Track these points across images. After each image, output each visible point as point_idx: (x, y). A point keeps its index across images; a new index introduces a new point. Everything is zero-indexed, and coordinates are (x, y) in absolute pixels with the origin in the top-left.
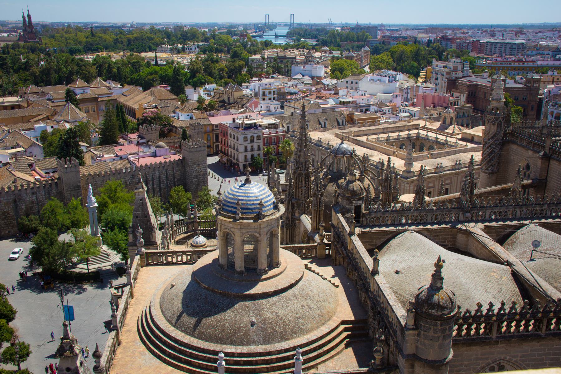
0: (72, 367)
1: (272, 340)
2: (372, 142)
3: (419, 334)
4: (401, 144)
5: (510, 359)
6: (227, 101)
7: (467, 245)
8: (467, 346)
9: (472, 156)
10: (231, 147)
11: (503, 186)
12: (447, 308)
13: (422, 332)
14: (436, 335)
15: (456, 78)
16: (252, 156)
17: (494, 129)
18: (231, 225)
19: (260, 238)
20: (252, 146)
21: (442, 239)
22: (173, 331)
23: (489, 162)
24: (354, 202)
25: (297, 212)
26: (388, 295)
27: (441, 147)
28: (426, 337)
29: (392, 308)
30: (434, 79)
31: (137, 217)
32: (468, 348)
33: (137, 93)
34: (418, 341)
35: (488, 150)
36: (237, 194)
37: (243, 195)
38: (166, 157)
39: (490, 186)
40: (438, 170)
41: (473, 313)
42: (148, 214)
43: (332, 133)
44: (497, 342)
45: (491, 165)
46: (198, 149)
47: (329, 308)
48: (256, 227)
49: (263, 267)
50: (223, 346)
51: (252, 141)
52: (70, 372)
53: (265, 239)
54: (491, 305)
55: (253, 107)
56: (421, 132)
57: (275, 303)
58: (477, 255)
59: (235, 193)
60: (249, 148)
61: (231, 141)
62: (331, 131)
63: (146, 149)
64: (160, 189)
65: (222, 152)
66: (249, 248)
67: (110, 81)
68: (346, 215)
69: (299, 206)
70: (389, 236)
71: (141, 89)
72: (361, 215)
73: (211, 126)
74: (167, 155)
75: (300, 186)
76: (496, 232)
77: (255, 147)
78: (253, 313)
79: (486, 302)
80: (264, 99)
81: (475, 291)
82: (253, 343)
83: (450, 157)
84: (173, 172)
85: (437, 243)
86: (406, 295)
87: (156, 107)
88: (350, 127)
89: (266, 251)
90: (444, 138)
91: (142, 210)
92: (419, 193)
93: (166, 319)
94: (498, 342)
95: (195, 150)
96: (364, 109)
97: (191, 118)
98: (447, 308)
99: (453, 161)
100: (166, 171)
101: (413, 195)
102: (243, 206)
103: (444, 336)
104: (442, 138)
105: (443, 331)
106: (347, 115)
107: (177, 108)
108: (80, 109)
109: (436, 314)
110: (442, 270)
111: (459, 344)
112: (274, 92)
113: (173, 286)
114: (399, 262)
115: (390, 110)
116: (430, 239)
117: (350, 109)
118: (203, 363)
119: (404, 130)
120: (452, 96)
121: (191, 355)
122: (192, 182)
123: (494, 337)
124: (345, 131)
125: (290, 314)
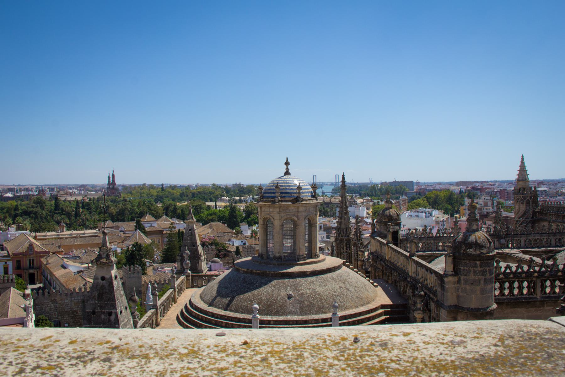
0: (107, 277)
1: (310, 311)
3: (459, 281)
13: (462, 277)
14: (477, 278)
28: (466, 281)
34: (458, 289)
49: (301, 253)
52: (104, 281)
75: (342, 251)
82: (290, 313)
98: (485, 247)
103: (485, 279)
105: (483, 273)
109: (474, 253)
125: (327, 292)
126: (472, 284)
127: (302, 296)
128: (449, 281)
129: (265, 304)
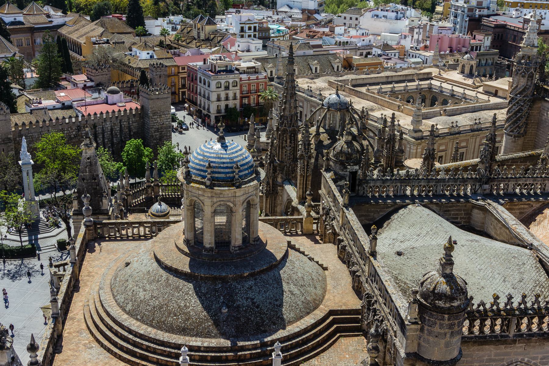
2: (374, 93)
3: (422, 330)
4: (408, 98)
5: (528, 361)
6: (196, 37)
7: (483, 223)
8: (479, 345)
9: (495, 114)
10: (200, 95)
11: (530, 153)
12: (457, 299)
13: (426, 327)
14: (442, 331)
15: (481, 16)
16: (227, 106)
17: (523, 82)
18: (200, 192)
19: (234, 210)
20: (227, 94)
21: (453, 214)
22: (126, 320)
23: (515, 122)
24: (349, 167)
25: (280, 176)
26: (386, 281)
27: (457, 101)
28: (430, 333)
29: (390, 297)
30: (452, 18)
31: (83, 179)
32: (480, 347)
33: (83, 22)
34: (420, 337)
35: (514, 107)
36: (208, 155)
37: (215, 155)
38: (120, 105)
39: (515, 152)
40: (453, 130)
41: (488, 306)
42: (98, 175)
43: (325, 81)
44: (514, 342)
45: (518, 126)
46: (159, 97)
47: (316, 294)
48: (230, 195)
50: (187, 338)
51: (227, 88)
53: (241, 210)
54: (510, 298)
55: (229, 46)
56: (433, 82)
57: (251, 287)
58: (495, 236)
59: (206, 154)
60: (223, 96)
61: (200, 87)
62: (324, 78)
63: (96, 95)
64: (113, 144)
65: (189, 100)
66: (221, 220)
67: (49, 7)
68: (339, 183)
69: (282, 170)
70: (390, 209)
71: (88, 18)
72: (357, 183)
73: (176, 68)
74: (121, 102)
75: (284, 145)
76: (519, 209)
77: (231, 95)
78: (224, 298)
79: (504, 293)
80: (242, 36)
81: (491, 279)
83: (467, 115)
84: (129, 123)
85: (447, 220)
86: (408, 282)
87: (107, 42)
88: (347, 74)
89: (241, 224)
90: (461, 90)
91: (90, 172)
92: (429, 158)
93: (118, 304)
94: (516, 340)
95: (157, 97)
96: (364, 54)
97: (151, 57)
99: (471, 119)
100: (120, 122)
101: (420, 161)
102: (215, 170)
103: (452, 332)
104: (459, 90)
105: (451, 326)
106: (344, 59)
107: (134, 44)
108: (11, 42)
109: (443, 305)
110: (452, 254)
111: (469, 342)
112: (255, 27)
113: (127, 264)
114: (401, 242)
115: (397, 54)
116: (439, 215)
117: (348, 52)
118: (162, 358)
119: (413, 81)
120: (474, 38)
121: (147, 349)
122: (153, 136)
123: (511, 336)
124: (340, 78)
125: (268, 301)
126: (436, 336)
127: (238, 311)
128: (411, 329)
129: (193, 322)
